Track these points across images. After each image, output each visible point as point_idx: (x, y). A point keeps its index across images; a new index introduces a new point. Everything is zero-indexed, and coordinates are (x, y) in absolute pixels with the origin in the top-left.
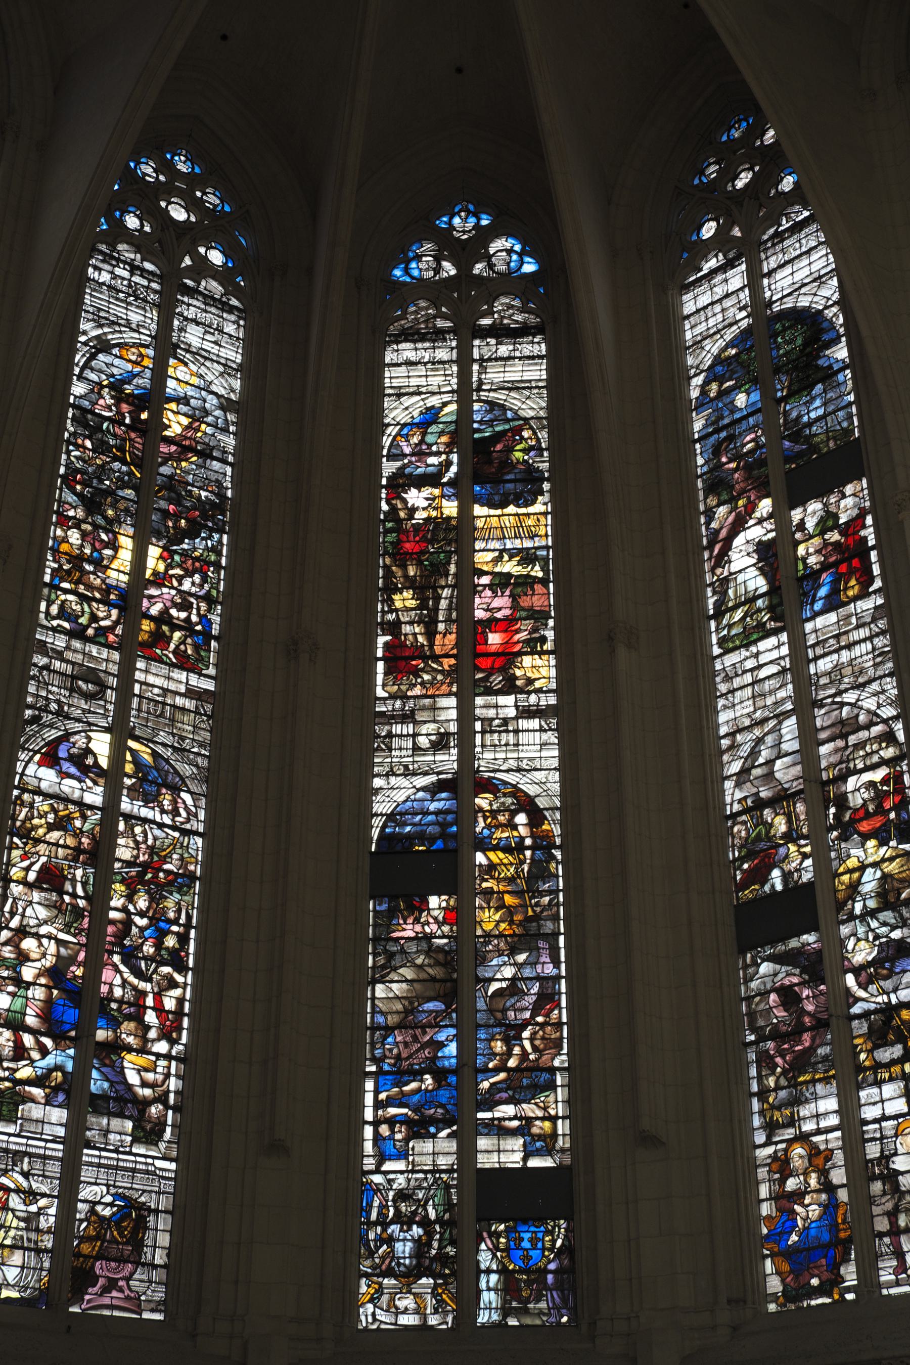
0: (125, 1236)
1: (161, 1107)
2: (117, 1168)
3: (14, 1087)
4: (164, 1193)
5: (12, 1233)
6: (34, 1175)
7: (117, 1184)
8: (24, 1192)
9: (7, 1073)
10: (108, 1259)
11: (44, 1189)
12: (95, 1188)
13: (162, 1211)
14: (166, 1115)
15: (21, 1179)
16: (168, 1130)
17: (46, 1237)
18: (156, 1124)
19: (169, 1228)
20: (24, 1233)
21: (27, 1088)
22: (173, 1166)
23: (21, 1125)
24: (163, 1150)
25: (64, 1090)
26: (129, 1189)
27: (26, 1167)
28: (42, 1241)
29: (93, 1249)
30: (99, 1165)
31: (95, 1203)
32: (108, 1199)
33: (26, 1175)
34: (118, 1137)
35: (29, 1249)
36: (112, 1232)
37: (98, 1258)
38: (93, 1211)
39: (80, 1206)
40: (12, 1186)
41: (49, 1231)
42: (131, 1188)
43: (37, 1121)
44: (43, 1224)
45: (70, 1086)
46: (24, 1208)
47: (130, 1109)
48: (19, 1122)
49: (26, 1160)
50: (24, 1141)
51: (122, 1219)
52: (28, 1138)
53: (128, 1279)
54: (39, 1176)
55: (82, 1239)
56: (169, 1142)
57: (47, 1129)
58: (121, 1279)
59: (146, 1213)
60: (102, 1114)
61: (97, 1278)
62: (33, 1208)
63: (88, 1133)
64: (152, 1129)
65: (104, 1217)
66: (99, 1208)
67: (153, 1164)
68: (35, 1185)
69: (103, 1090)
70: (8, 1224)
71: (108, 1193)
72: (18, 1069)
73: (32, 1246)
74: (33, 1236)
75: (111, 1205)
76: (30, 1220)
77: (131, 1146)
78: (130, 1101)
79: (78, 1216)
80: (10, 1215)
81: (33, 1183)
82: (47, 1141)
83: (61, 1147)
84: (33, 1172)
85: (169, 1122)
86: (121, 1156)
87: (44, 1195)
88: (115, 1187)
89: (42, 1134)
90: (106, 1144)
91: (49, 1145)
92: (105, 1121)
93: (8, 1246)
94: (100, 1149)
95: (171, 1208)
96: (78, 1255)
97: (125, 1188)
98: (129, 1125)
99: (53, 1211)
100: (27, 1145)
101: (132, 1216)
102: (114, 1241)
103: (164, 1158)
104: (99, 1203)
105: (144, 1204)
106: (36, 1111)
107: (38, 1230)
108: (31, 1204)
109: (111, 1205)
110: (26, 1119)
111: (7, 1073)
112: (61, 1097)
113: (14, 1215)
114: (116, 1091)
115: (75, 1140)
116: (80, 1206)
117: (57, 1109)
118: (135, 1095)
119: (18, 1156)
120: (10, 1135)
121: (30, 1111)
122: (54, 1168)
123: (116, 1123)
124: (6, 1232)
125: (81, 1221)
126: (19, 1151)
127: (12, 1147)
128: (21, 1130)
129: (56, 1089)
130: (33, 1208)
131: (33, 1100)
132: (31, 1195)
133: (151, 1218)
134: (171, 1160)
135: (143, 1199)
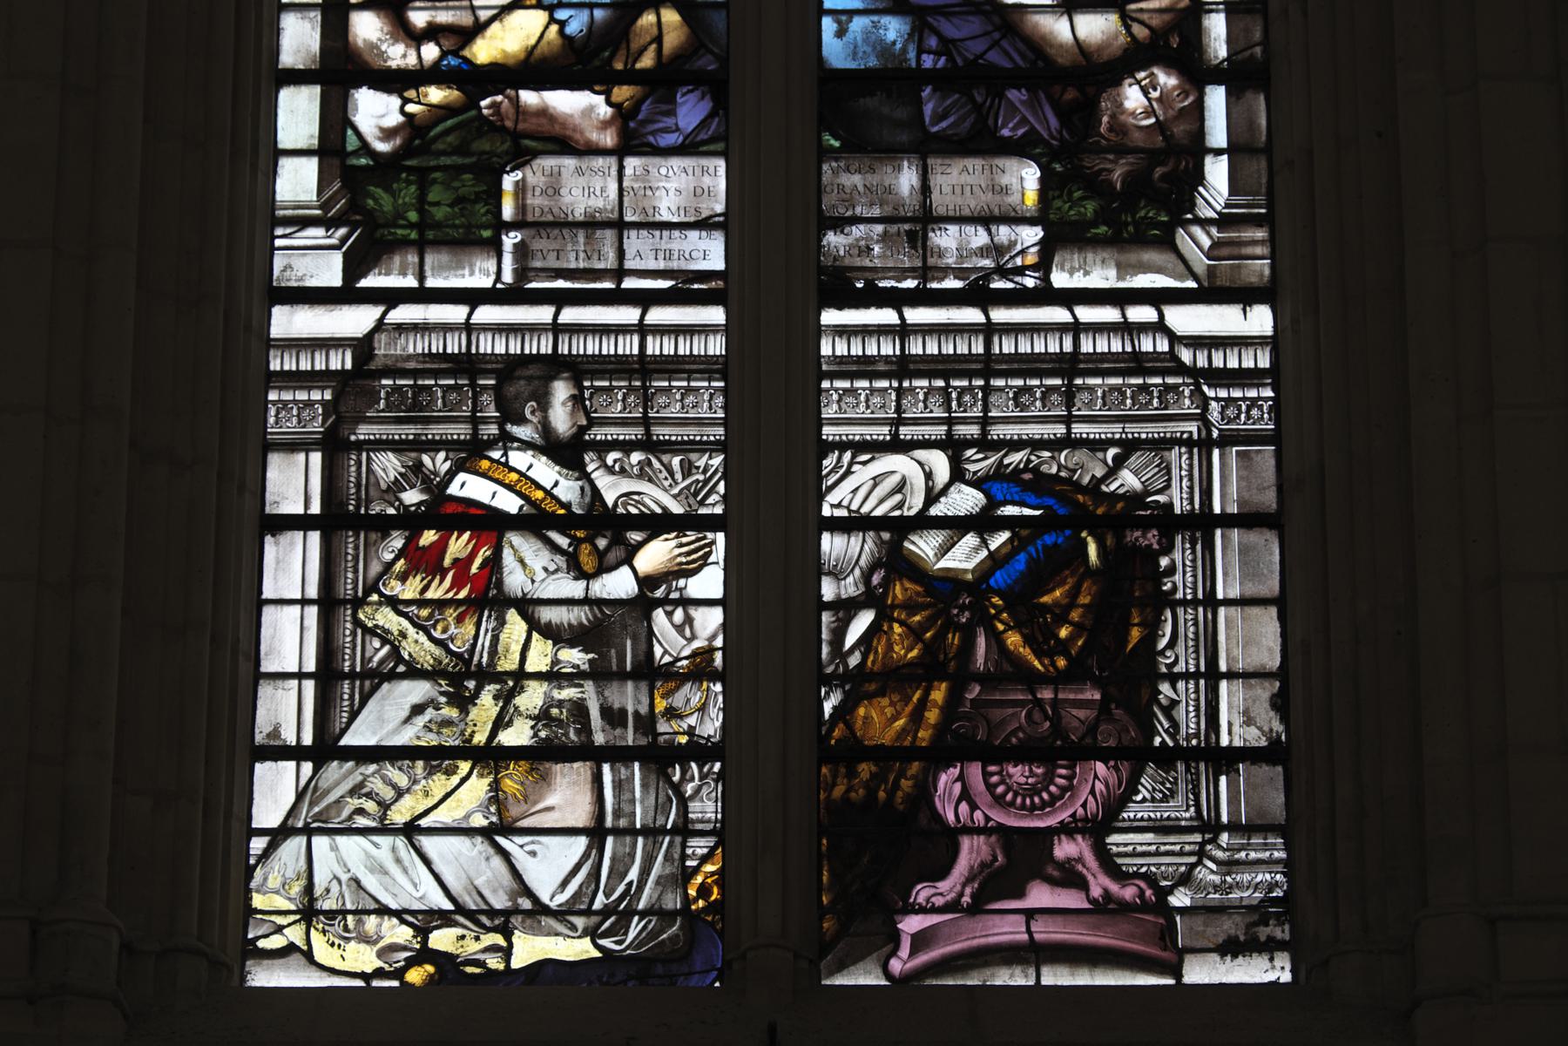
0: (1063, 647)
1: (1167, 80)
2: (988, 366)
3: (472, 102)
4: (1226, 440)
5: (532, 697)
6: (603, 447)
7: (998, 432)
8: (567, 522)
9: (430, 52)
10: (994, 754)
11: (660, 498)
12: (898, 464)
13: (1227, 521)
14: (1199, 108)
15: (545, 472)
16: (1217, 172)
17: (689, 695)
18: (1154, 156)
19: (1272, 586)
20: (589, 693)
21: (528, 97)
22: (1260, 320)
23: (521, 250)
24: (1200, 262)
25: (697, 81)
26: (1055, 445)
27: (561, 419)
28: (672, 713)
29: (917, 717)
30: (903, 367)
31: (902, 527)
32: (965, 500)
33: (567, 453)
34: (979, 237)
35: (617, 755)
36: (996, 639)
37: (942, 753)
38: (895, 562)
39: (832, 545)
40: (509, 503)
41: (700, 668)
42: (1069, 442)
43: (591, 224)
44: (669, 640)
45: (724, 61)
46: (576, 589)
47: (1019, 111)
48: (510, 240)
49: (561, 391)
50: (543, 314)
51: (1039, 578)
52: (560, 299)
53: (1098, 828)
54: (627, 447)
55: (859, 686)
56: (1224, 221)
57: (641, 250)
58: (1066, 830)
59: (1152, 538)
60: (892, 153)
61: (950, 838)
62: (619, 584)
63: (832, 239)
64: (1138, 185)
65: (951, 580)
66: (924, 545)
67: (1160, 327)
68: (611, 489)
69: (884, 50)
70: (508, 664)
71: (957, 475)
72: (479, 28)
73: (630, 738)
74: (629, 697)
75: (982, 523)
76: (611, 636)
77: (1044, 266)
78: (1015, 78)
79: (828, 590)
80: (516, 626)
81: (602, 480)
82: (645, 299)
83: (715, 315)
84: (599, 434)
85: (1218, 135)
86: (1000, 315)
87: (658, 524)
88: (985, 444)
89: (620, 273)
90: (925, 273)
91: (659, 315)
92: (907, 180)
93: (517, 753)
94: (897, 300)
95: (1268, 499)
96: (854, 751)
97: (1036, 445)
98: (1025, 180)
99: (709, 583)
100: (556, 329)
101: (1087, 568)
102: (1009, 670)
103: (1210, 293)
104: (923, 522)
105: (1135, 499)
106: (586, 188)
107: (649, 672)
108: (603, 568)
109: (982, 523)
110: (539, 226)
111: (430, 52)
112: (690, 112)
113: (534, 625)
114: (947, 46)
115: (778, 276)
116: (832, 545)
117: (676, 163)
118: (1038, 47)
119: (519, 380)
120: (472, 298)
121: (554, 190)
122: (699, 407)
123: (957, 180)
124: (506, 697)
125: (846, 609)
126: (524, 360)
127: (487, 345)
128: (522, 273)
129: (664, 82)
130: (619, 584)
131: (562, 140)
132: (599, 532)
133: (1180, 554)
134: (1244, 296)
135: (1128, 480)
